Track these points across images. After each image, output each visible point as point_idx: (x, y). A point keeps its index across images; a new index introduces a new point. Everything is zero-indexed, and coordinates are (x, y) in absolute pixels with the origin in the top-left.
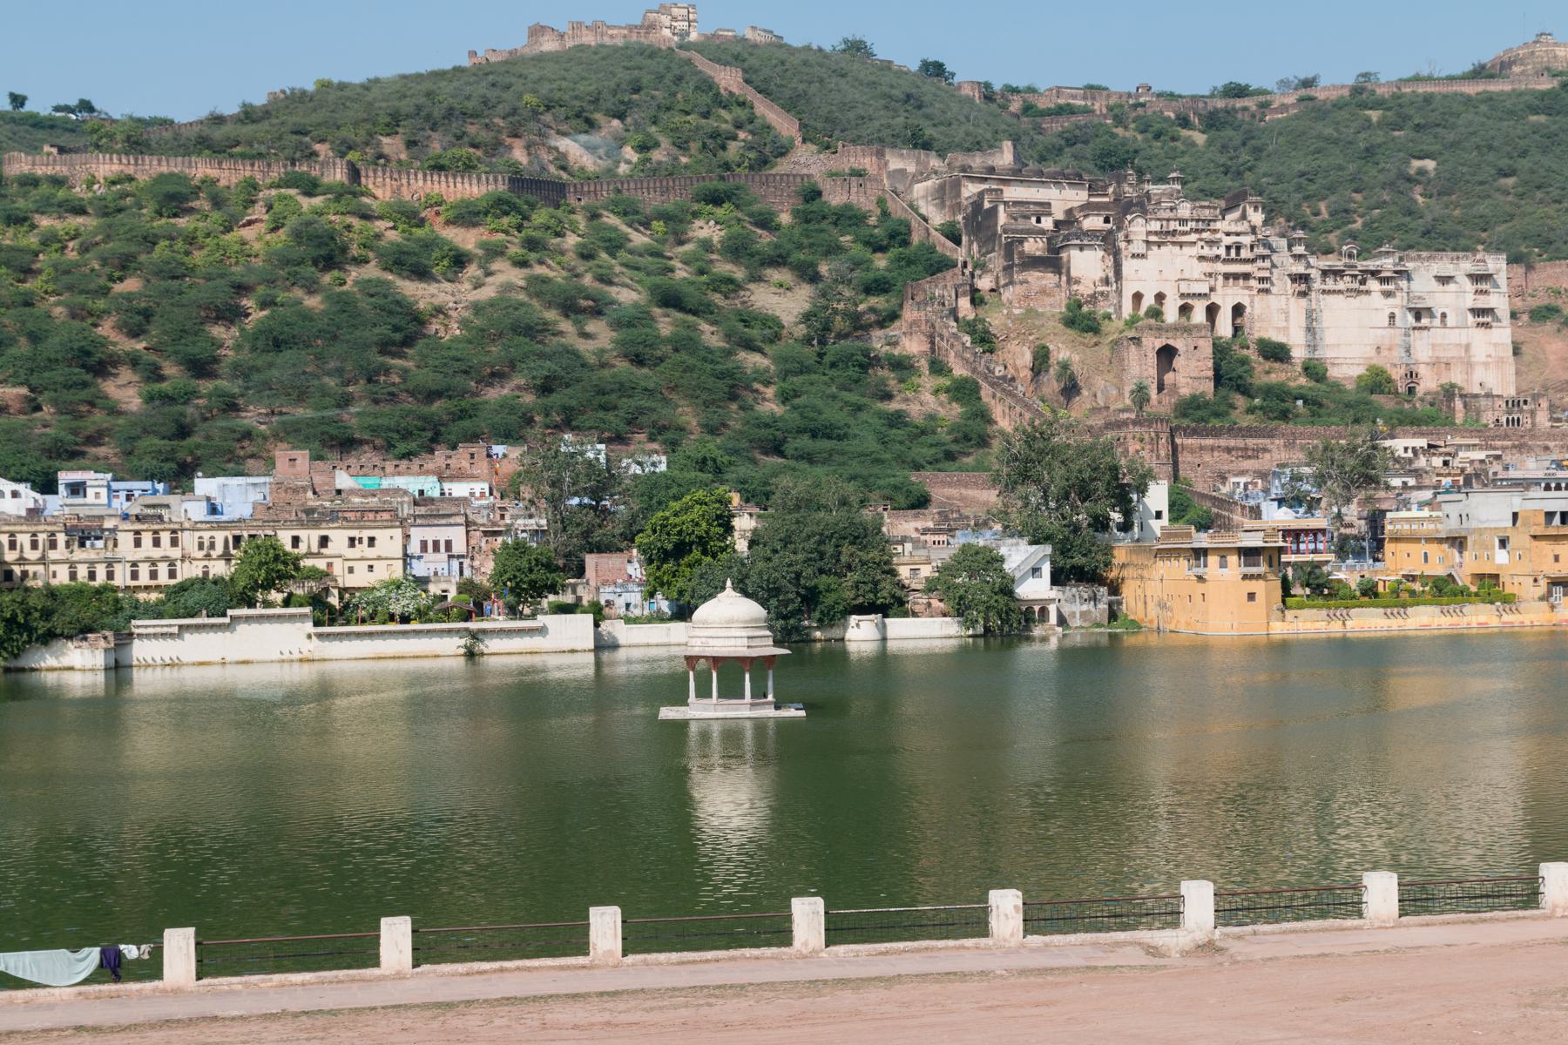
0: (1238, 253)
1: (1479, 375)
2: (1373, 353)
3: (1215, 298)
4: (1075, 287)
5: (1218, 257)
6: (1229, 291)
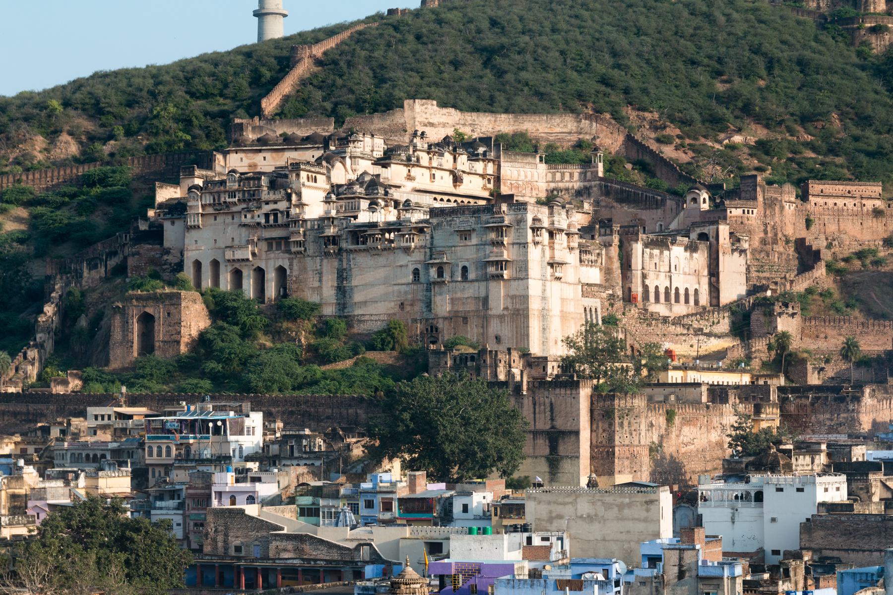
0: (276, 220)
1: (494, 327)
2: (397, 309)
4: (165, 257)
5: (259, 224)
6: (272, 255)
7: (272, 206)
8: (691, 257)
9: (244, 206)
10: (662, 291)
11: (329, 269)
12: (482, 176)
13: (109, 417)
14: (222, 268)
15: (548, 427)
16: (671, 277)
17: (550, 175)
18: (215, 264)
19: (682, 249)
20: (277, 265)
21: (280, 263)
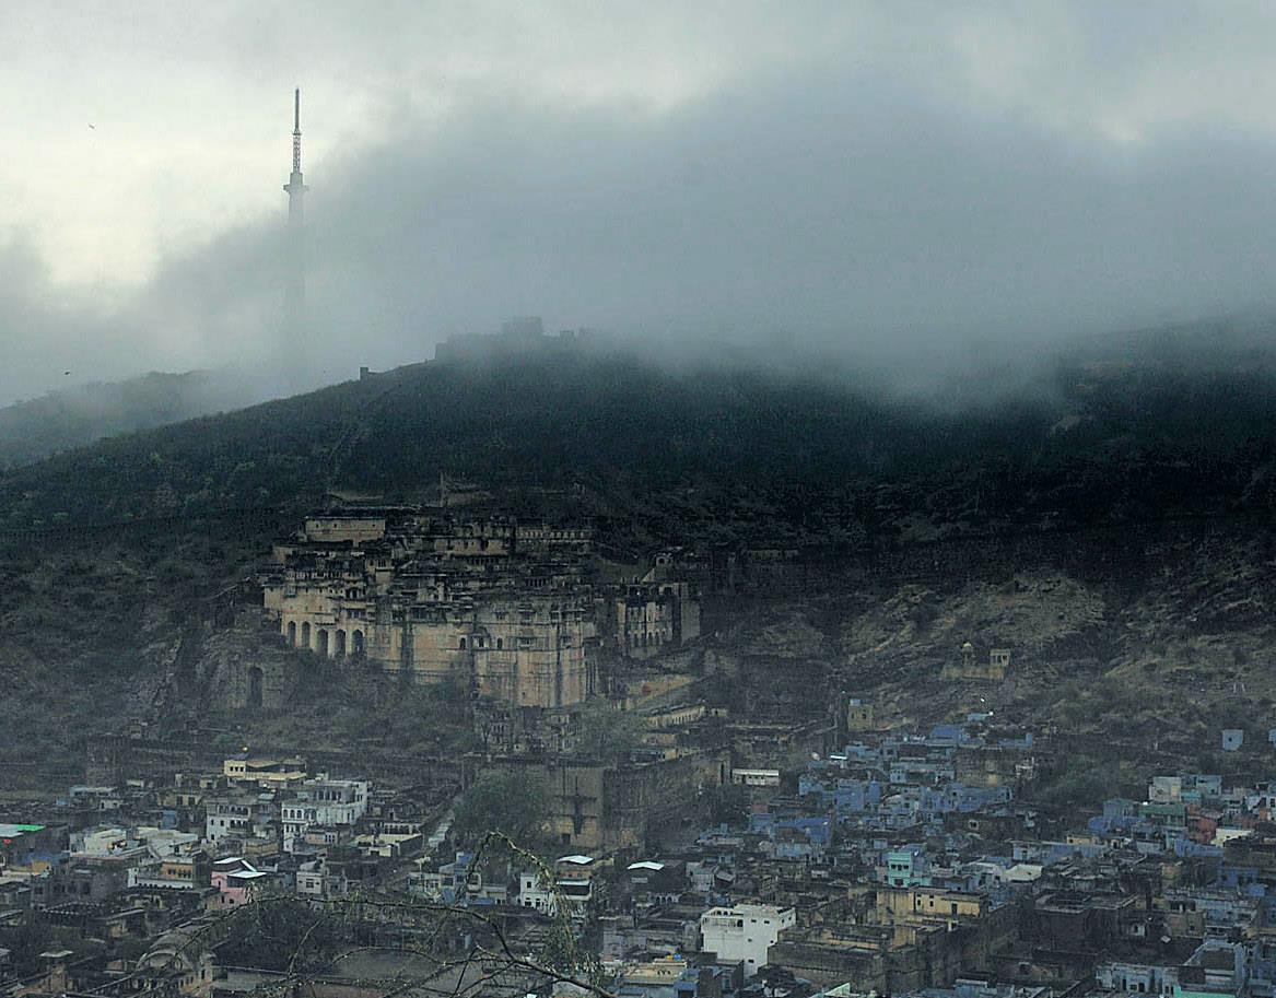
0: (355, 595)
3: (339, 627)
5: (341, 597)
7: (352, 585)
8: (661, 609)
9: (329, 583)
10: (639, 636)
11: (395, 634)
12: (502, 538)
13: (242, 769)
14: (312, 629)
15: (574, 794)
16: (645, 627)
17: (552, 534)
18: (306, 625)
19: (654, 604)
20: (356, 629)
21: (357, 628)
